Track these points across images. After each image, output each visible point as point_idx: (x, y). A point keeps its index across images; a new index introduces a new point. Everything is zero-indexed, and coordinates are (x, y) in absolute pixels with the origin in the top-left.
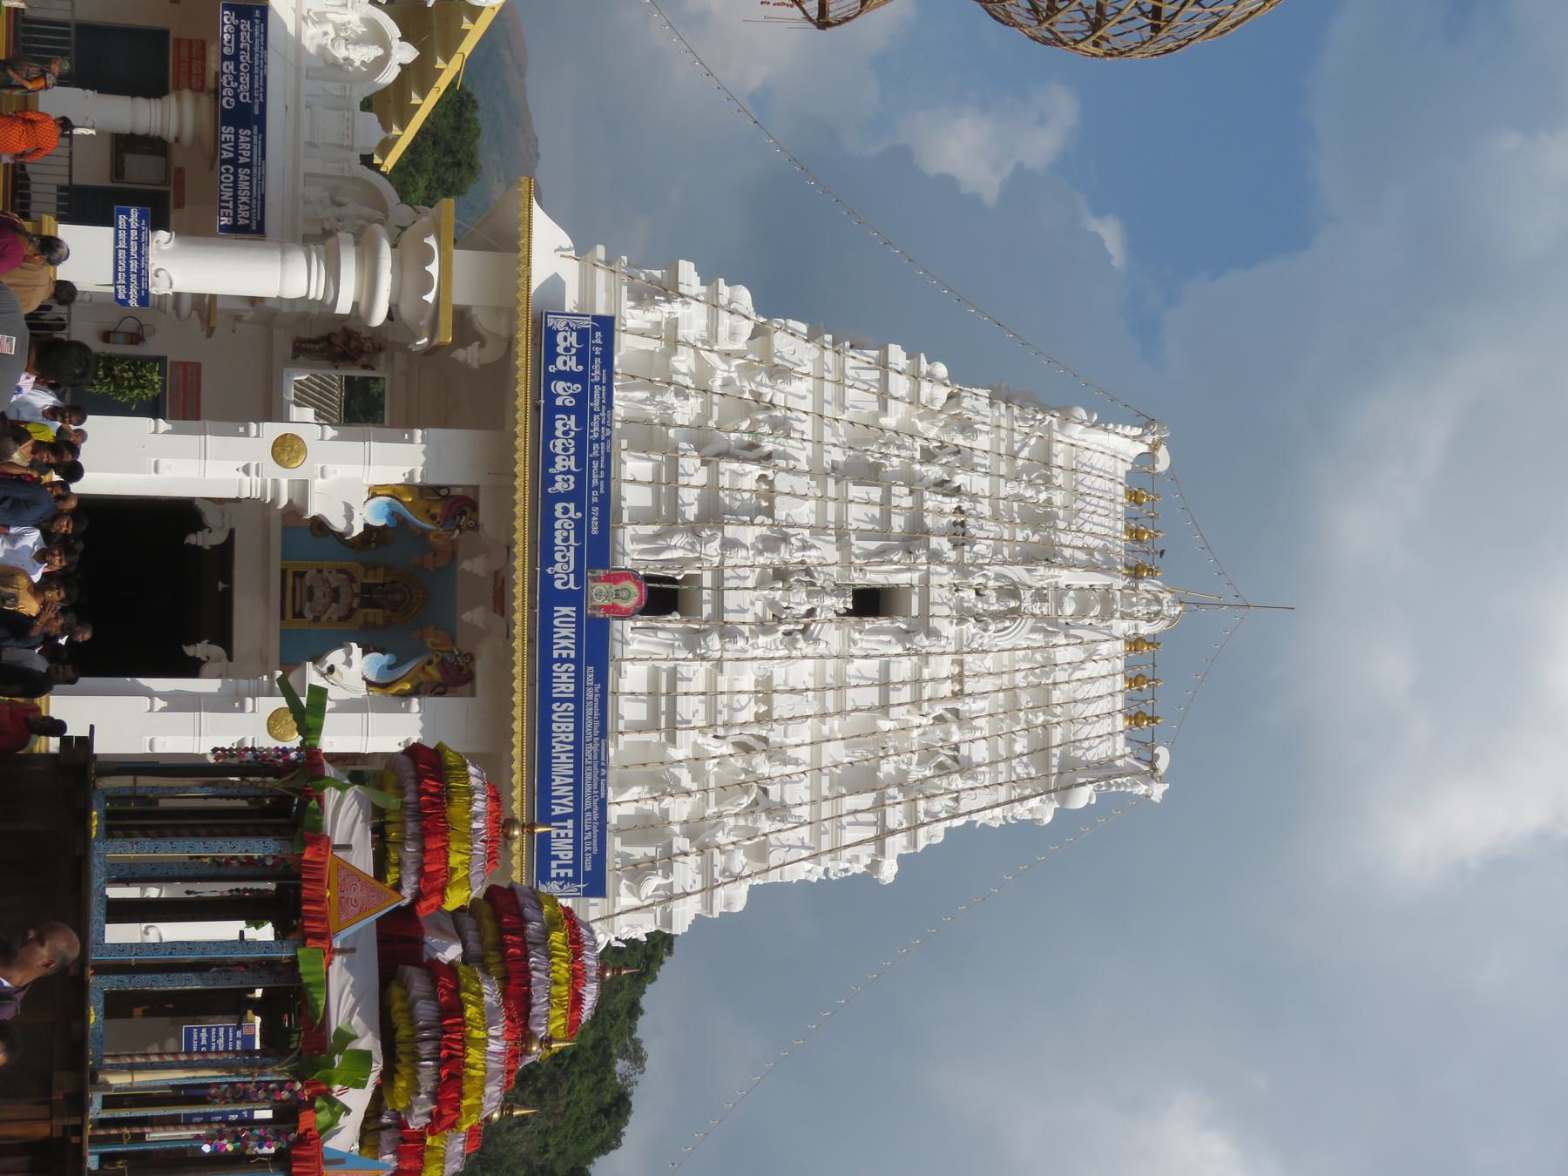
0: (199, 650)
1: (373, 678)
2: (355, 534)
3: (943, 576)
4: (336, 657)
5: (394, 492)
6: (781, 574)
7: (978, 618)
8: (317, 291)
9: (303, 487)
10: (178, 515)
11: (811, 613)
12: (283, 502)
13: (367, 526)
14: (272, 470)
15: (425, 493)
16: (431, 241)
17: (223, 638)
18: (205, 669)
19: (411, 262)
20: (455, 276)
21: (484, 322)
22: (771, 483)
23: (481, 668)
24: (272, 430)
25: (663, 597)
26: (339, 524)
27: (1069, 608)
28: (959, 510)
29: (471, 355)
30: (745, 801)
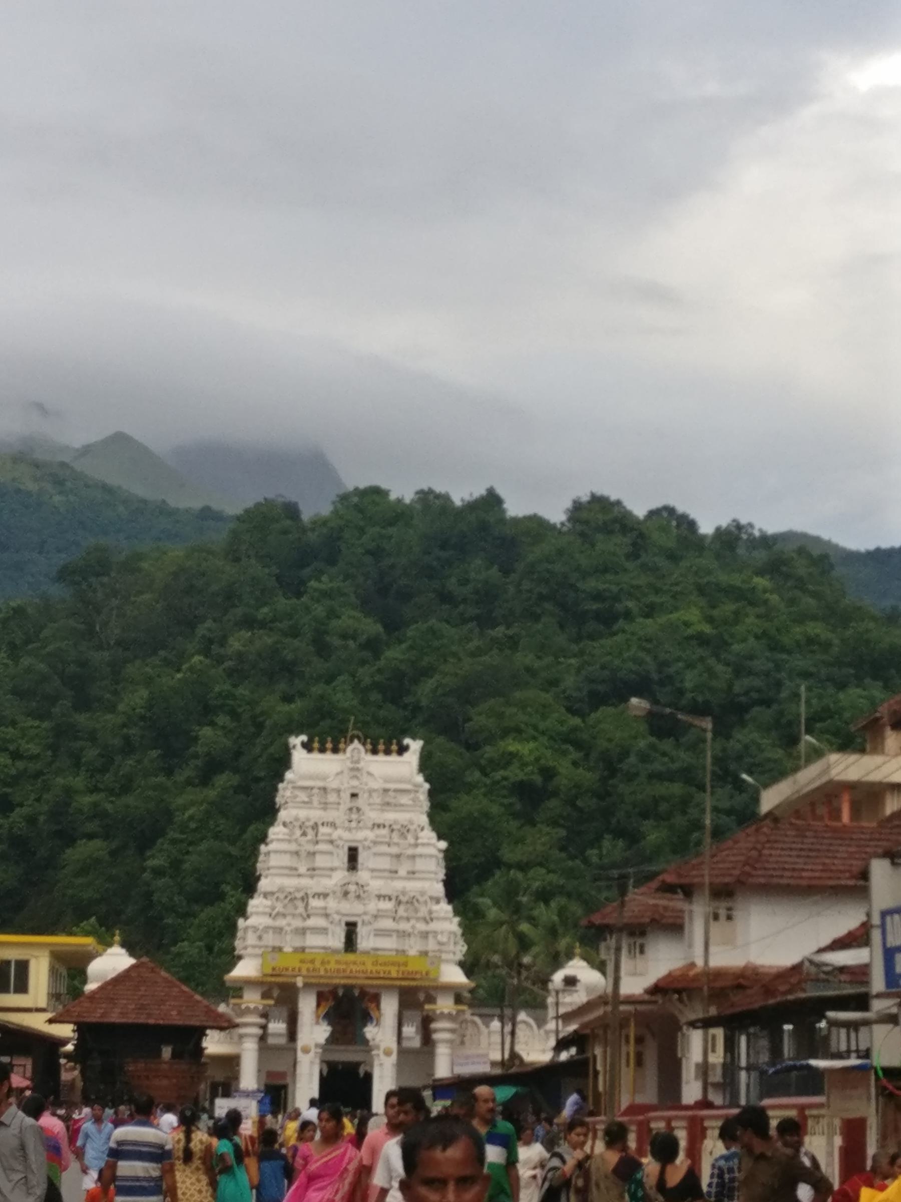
3: (346, 835)
4: (369, 1036)
6: (346, 894)
7: (359, 822)
8: (256, 1040)
9: (317, 1046)
10: (325, 1082)
11: (357, 884)
14: (312, 1054)
15: (318, 1005)
16: (243, 1007)
17: (358, 1065)
18: (368, 1068)
19: (248, 1011)
20: (252, 999)
21: (265, 988)
23: (372, 991)
24: (300, 1054)
26: (326, 1035)
27: (355, 783)
28: (323, 824)
29: (276, 993)
30: (416, 904)
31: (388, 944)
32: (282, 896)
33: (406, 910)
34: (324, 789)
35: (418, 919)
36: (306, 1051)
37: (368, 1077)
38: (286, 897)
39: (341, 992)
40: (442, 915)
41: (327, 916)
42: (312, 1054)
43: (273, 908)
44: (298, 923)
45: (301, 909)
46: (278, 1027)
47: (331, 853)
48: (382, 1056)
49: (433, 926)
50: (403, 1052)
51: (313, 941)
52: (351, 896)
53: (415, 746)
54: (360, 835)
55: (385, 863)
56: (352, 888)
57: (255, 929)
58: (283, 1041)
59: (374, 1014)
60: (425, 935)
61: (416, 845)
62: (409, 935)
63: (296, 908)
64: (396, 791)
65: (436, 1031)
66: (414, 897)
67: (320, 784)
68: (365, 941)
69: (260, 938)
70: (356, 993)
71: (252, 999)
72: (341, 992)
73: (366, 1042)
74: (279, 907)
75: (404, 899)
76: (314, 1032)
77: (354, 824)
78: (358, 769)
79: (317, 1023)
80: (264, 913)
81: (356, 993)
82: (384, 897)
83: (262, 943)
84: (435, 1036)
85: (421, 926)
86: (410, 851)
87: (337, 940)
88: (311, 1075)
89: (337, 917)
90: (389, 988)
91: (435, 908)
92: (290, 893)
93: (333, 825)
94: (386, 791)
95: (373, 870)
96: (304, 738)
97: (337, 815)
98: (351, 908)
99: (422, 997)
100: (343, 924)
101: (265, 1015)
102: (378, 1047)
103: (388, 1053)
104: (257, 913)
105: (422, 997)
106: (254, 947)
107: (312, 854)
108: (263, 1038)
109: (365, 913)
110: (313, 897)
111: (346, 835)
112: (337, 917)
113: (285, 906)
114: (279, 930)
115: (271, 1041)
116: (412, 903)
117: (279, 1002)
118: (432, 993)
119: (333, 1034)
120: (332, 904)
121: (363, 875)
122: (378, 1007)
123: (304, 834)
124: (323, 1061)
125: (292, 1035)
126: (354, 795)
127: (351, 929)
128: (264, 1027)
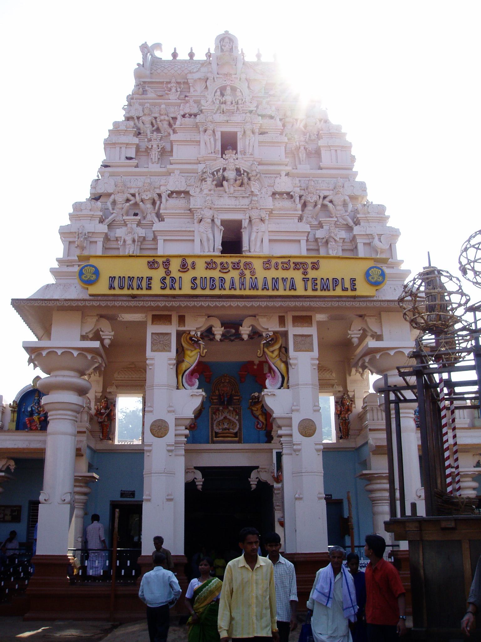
1: (279, 384)
2: (204, 394)
4: (270, 402)
12: (187, 432)
13: (198, 388)
14: (170, 437)
21: (89, 327)
22: (172, 192)
25: (232, 243)
26: (197, 402)
30: (330, 205)
32: (120, 198)
38: (128, 200)
48: (297, 437)
59: (277, 364)
62: (327, 242)
66: (325, 198)
68: (256, 243)
74: (116, 215)
75: (311, 199)
80: (92, 217)
82: (281, 194)
87: (209, 241)
89: (208, 214)
92: (134, 195)
98: (229, 205)
100: (218, 222)
110: (169, 196)
116: (324, 206)
127: (232, 243)
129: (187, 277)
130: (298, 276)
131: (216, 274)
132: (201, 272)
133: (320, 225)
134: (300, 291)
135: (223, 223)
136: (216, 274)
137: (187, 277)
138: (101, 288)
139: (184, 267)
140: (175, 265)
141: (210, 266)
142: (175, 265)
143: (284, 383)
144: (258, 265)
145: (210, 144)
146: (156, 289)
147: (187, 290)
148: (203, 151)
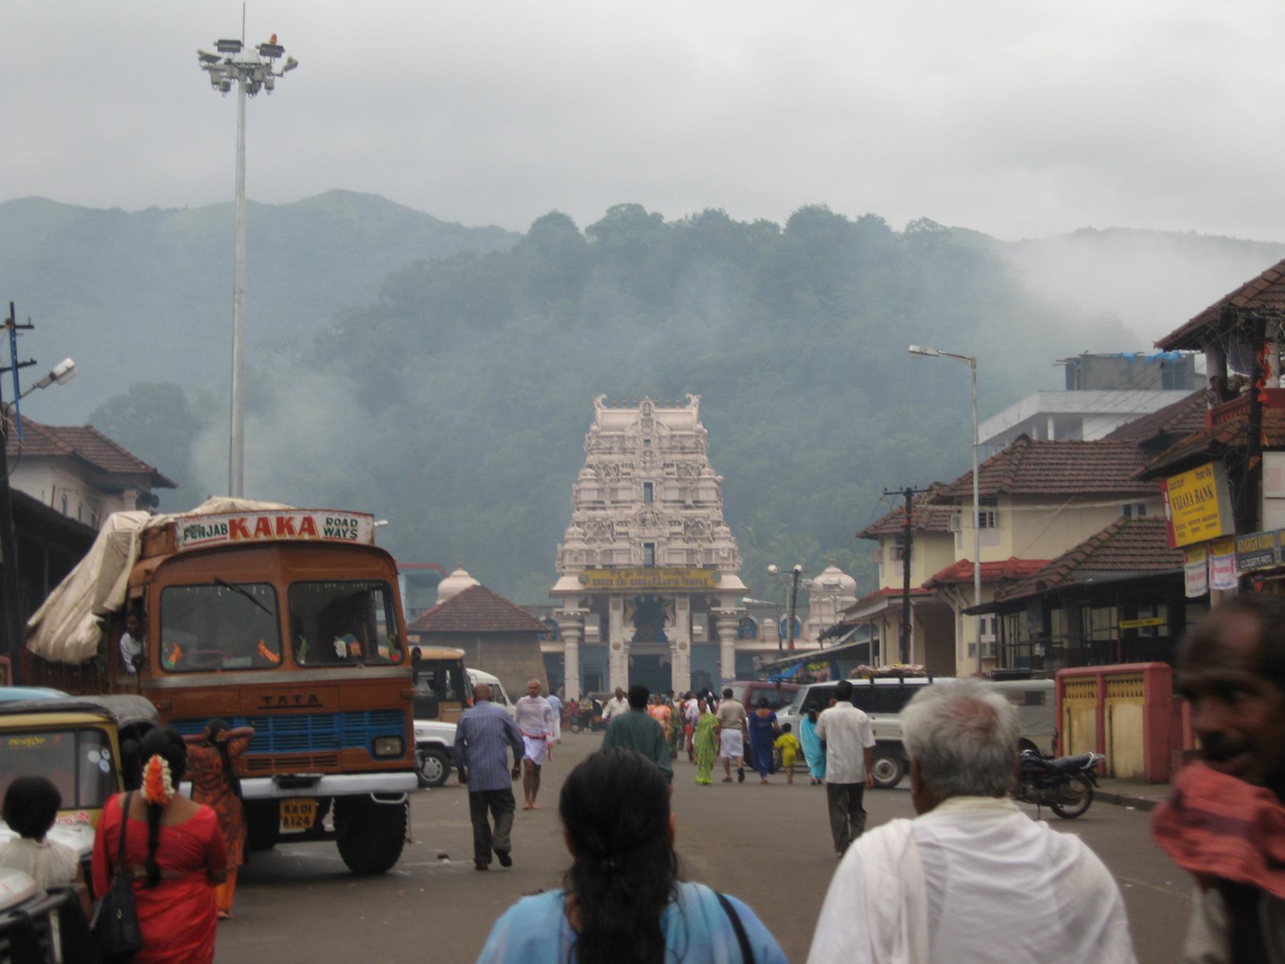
0: (661, 663)
3: (643, 474)
5: (624, 619)
6: (644, 521)
14: (621, 650)
17: (658, 657)
24: (612, 650)
26: (633, 634)
29: (590, 602)
31: (679, 560)
32: (592, 524)
33: (693, 533)
34: (623, 437)
35: (703, 540)
36: (617, 647)
37: (668, 667)
39: (643, 600)
40: (722, 535)
41: (629, 539)
42: (621, 650)
43: (585, 535)
44: (606, 546)
45: (609, 535)
46: (592, 629)
47: (630, 489)
49: (713, 545)
50: (694, 646)
51: (620, 560)
52: (648, 524)
53: (695, 400)
54: (654, 474)
55: (674, 495)
56: (649, 516)
57: (571, 552)
58: (597, 640)
59: (670, 616)
60: (709, 551)
61: (699, 480)
63: (604, 533)
64: (681, 436)
65: (720, 628)
67: (620, 433)
69: (576, 559)
70: (655, 599)
71: (572, 609)
72: (643, 600)
73: (665, 639)
76: (622, 633)
77: (648, 465)
78: (651, 420)
79: (625, 625)
81: (655, 599)
83: (579, 563)
84: (723, 632)
85: (706, 545)
86: (694, 486)
88: (621, 666)
90: (682, 595)
91: (717, 529)
93: (632, 466)
94: (673, 437)
95: (665, 501)
96: (604, 396)
97: (636, 459)
98: (651, 533)
99: (708, 601)
101: (581, 620)
102: (674, 643)
103: (683, 647)
104: (573, 539)
105: (708, 601)
106: (571, 566)
107: (614, 490)
108: (581, 639)
109: (661, 536)
111: (643, 474)
112: (637, 540)
113: (595, 534)
114: (590, 553)
115: (587, 641)
117: (593, 610)
118: (717, 597)
119: (637, 634)
120: (633, 530)
121: (658, 506)
122: (674, 611)
123: (608, 474)
124: (630, 656)
125: (605, 634)
126: (647, 441)
128: (582, 630)
129: (629, 579)
130: (680, 578)
131: (642, 578)
132: (635, 576)
133: (695, 540)
134: (681, 585)
135: (647, 545)
136: (642, 578)
137: (629, 579)
138: (591, 586)
139: (627, 575)
140: (623, 574)
141: (639, 574)
142: (623, 574)
143: (674, 624)
144: (661, 573)
145: (638, 492)
146: (615, 586)
147: (629, 585)
148: (634, 496)
